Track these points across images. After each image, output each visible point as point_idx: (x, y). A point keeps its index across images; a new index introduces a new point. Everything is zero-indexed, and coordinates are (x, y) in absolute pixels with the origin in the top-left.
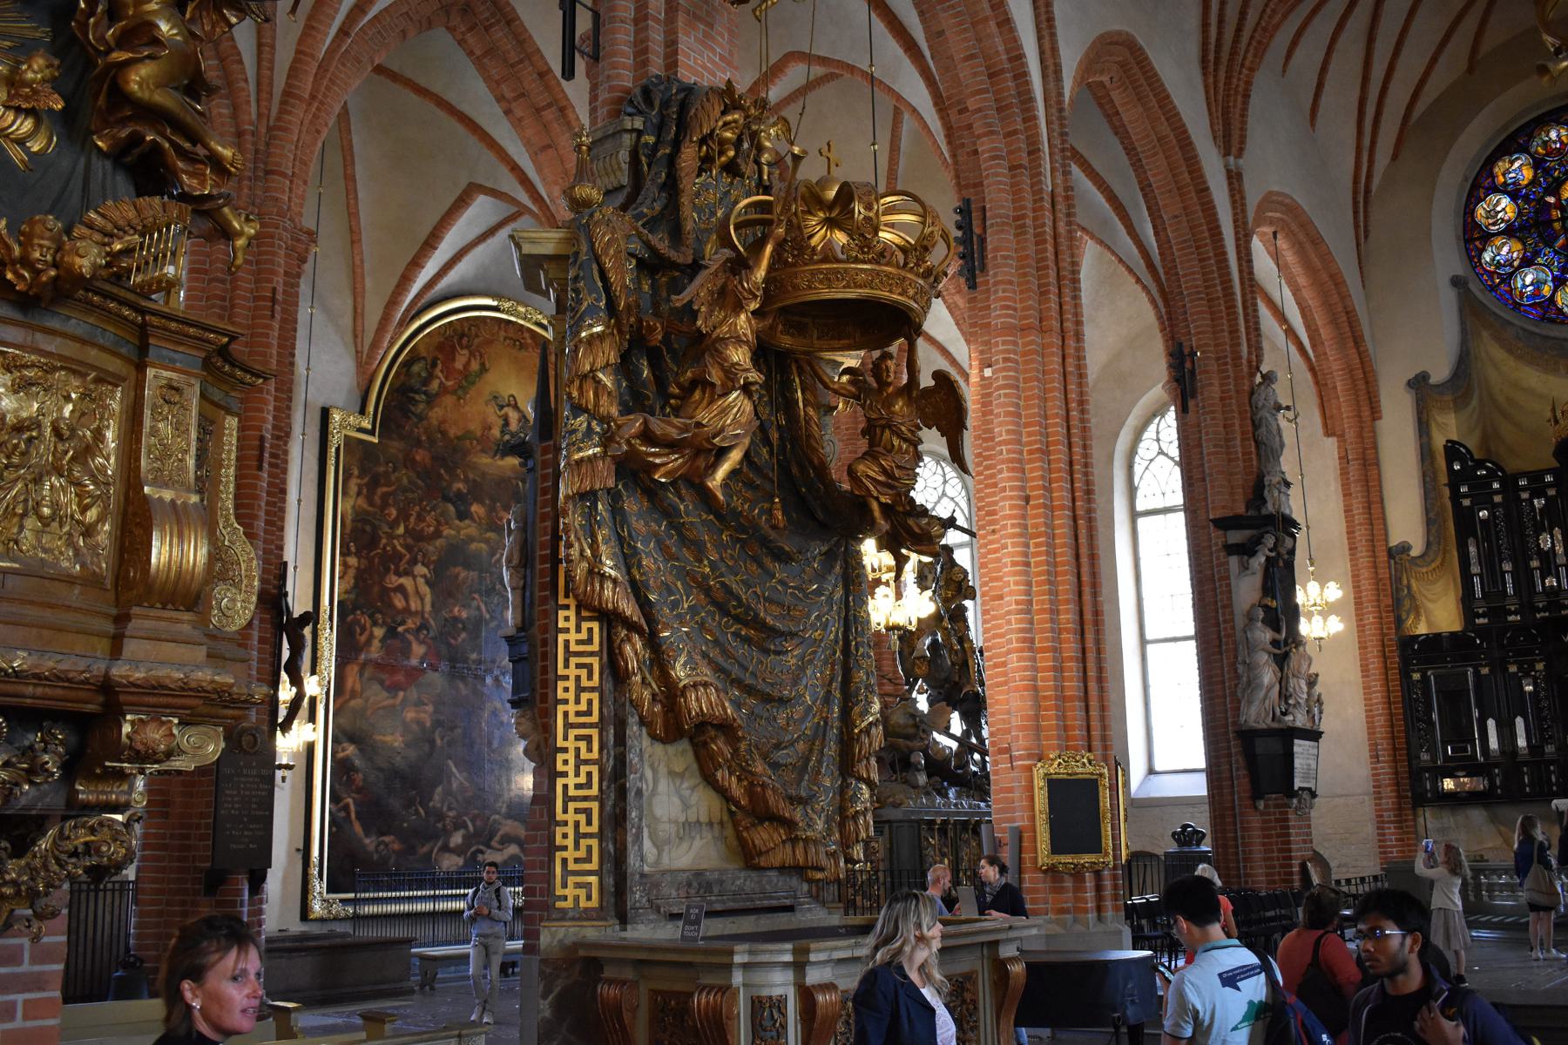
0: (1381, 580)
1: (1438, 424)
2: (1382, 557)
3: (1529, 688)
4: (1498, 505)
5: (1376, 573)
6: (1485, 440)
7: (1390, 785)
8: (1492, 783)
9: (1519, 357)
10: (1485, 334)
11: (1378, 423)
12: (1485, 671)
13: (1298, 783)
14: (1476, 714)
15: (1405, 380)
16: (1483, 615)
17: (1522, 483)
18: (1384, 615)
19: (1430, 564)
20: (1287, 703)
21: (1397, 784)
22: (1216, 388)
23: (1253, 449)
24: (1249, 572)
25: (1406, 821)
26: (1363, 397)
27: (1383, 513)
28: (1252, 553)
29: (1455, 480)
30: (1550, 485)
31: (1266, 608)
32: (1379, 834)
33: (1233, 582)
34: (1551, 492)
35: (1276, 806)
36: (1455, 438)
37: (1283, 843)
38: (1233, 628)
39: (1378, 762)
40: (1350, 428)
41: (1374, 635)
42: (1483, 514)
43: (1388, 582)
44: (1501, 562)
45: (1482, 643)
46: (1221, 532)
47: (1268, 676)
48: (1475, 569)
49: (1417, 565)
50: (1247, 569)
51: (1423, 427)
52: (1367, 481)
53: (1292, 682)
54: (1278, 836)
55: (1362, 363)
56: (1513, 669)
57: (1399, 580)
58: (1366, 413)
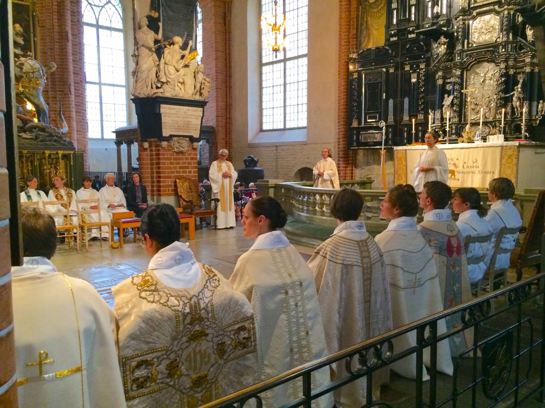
12: (392, 71)
43: (355, 20)
45: (392, 53)
49: (373, 8)
56: (407, 68)
57: (362, 18)
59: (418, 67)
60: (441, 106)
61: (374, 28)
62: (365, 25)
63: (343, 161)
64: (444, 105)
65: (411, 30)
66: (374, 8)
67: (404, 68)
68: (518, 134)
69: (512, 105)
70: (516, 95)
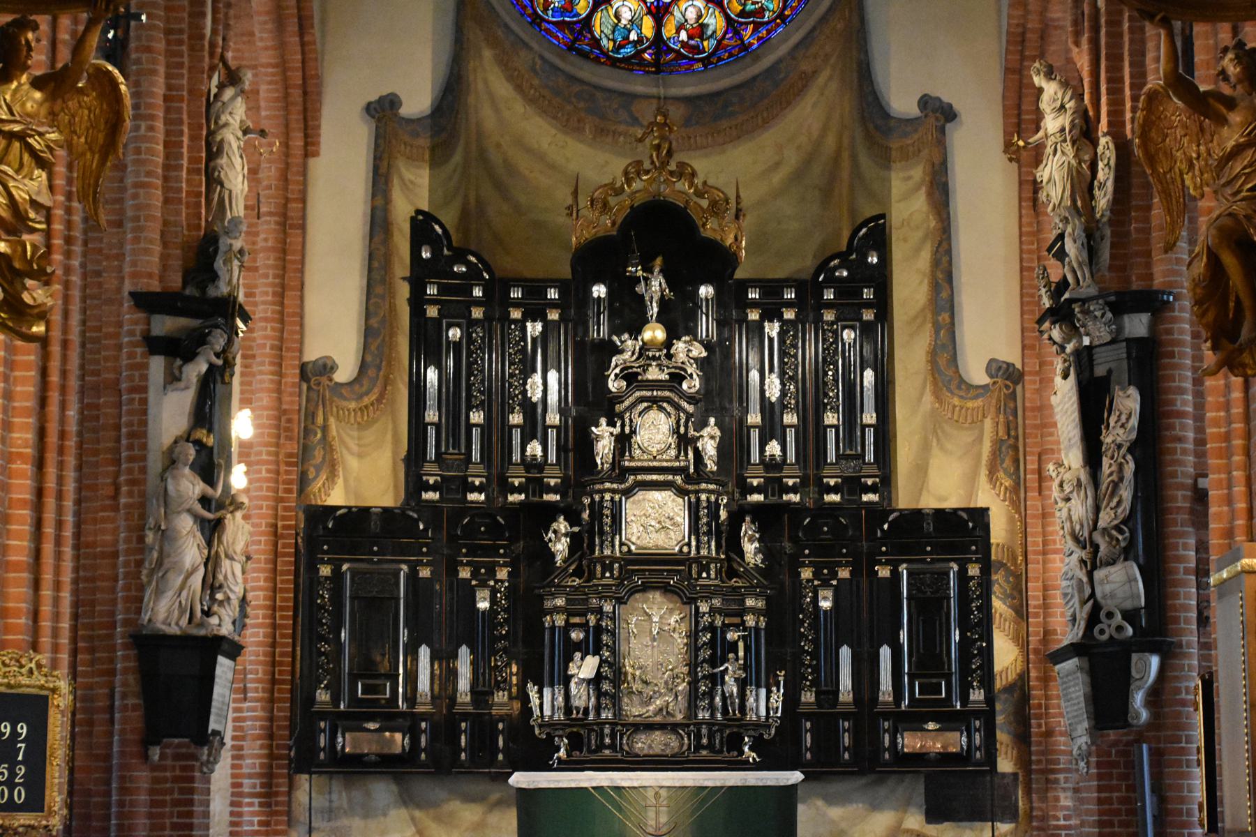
0: (285, 412)
1: (402, 179)
2: (292, 375)
3: (483, 605)
4: (477, 321)
5: (279, 400)
6: (465, 215)
7: (259, 737)
8: (415, 741)
9: (531, 101)
10: (487, 54)
11: (312, 162)
13: (213, 725)
14: (403, 635)
15: (363, 103)
16: (434, 488)
17: (516, 294)
18: (283, 468)
19: (360, 397)
20: (213, 599)
21: (271, 736)
22: (161, 80)
23: (203, 189)
24: (182, 384)
25: (277, 794)
26: (295, 116)
27: (302, 306)
28: (189, 357)
29: (419, 275)
30: (553, 305)
31: (198, 443)
32: (232, 814)
33: (152, 396)
34: (553, 316)
35: (177, 757)
36: (425, 208)
37: (180, 815)
38: (143, 470)
39: (245, 699)
40: (269, 161)
41: (266, 498)
42: (455, 333)
43: (296, 417)
44: (469, 408)
45: (426, 530)
46: (141, 315)
47: (191, 551)
48: (431, 415)
50: (179, 379)
51: (380, 180)
52: (284, 252)
53: (226, 564)
54: (176, 803)
55: (303, 62)
56: (465, 573)
57: (310, 416)
58: (297, 142)
59: (491, 573)
60: (566, 680)
61: (348, 449)
62: (319, 436)
63: (261, 805)
64: (572, 676)
65: (477, 483)
66: (345, 399)
67: (457, 572)
68: (735, 753)
69: (723, 690)
70: (730, 668)
